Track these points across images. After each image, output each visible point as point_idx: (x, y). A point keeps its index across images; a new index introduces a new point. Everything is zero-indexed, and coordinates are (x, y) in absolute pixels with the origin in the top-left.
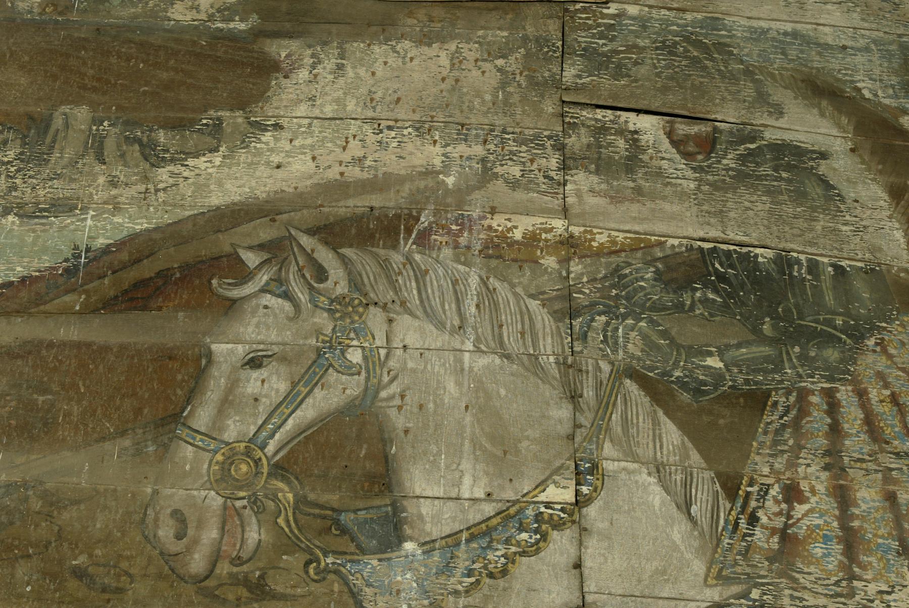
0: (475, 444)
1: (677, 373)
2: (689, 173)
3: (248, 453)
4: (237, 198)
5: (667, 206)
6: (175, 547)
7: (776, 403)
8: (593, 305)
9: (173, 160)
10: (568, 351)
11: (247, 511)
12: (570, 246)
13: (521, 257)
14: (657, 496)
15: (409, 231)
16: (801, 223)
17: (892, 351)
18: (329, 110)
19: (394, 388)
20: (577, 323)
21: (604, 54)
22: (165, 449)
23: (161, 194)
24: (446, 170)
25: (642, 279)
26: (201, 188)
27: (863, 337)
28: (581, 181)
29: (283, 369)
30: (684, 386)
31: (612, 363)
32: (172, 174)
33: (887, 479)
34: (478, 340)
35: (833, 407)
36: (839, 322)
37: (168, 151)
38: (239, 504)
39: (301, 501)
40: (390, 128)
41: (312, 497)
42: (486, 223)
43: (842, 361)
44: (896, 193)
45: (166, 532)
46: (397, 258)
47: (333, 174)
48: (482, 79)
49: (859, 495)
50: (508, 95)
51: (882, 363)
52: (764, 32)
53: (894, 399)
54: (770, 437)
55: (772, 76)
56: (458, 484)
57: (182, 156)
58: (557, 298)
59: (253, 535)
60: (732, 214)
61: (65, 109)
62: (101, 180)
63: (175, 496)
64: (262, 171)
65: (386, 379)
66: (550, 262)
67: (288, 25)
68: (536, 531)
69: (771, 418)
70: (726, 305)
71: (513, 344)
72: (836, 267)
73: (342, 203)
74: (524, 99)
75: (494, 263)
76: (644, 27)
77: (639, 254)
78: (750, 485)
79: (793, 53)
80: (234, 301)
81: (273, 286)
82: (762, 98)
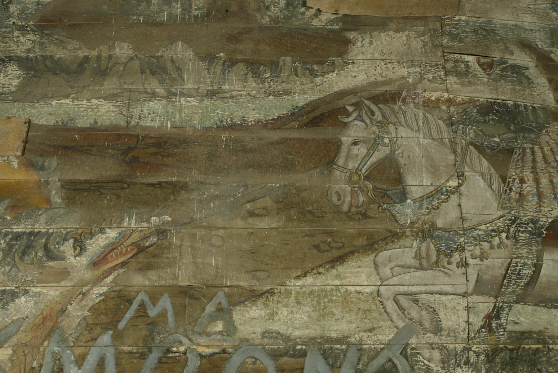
0: (426, 168)
1: (486, 143)
2: (485, 76)
3: (356, 173)
4: (343, 88)
5: (479, 87)
6: (338, 203)
7: (516, 152)
8: (458, 121)
9: (320, 75)
10: (452, 137)
11: (359, 191)
12: (450, 102)
13: (435, 106)
14: (482, 183)
15: (399, 98)
16: (521, 92)
17: (550, 134)
18: (369, 57)
19: (400, 151)
20: (454, 127)
21: (455, 34)
22: (330, 173)
23: (318, 87)
24: (409, 77)
25: (473, 112)
26: (330, 85)
27: (541, 130)
28: (452, 79)
29: (364, 145)
30: (488, 147)
31: (465, 141)
32: (321, 80)
33: (550, 176)
34: (424, 134)
35: (533, 153)
36: (534, 125)
37: (318, 72)
38: (356, 189)
39: (375, 188)
40: (389, 63)
41: (378, 186)
42: (423, 95)
43: (535, 138)
44: (550, 81)
45: (335, 199)
46: (396, 107)
47: (373, 79)
48: (417, 44)
49: (542, 181)
50: (426, 50)
51: (547, 138)
52: (506, 25)
53: (551, 150)
54: (515, 163)
55: (509, 40)
56: (422, 181)
58: (447, 119)
59: (361, 199)
60: (500, 90)
61: (283, 58)
62: (298, 83)
63: (336, 187)
64: (350, 78)
65: (397, 148)
66: (444, 107)
67: (352, 27)
68: (447, 195)
69: (515, 157)
70: (499, 121)
71: (435, 135)
72: (532, 107)
73: (377, 89)
74: (431, 51)
75: (427, 108)
76: (467, 24)
77: (471, 104)
78: (510, 179)
79: (516, 32)
80: (346, 123)
81: (358, 118)
82: (507, 49)
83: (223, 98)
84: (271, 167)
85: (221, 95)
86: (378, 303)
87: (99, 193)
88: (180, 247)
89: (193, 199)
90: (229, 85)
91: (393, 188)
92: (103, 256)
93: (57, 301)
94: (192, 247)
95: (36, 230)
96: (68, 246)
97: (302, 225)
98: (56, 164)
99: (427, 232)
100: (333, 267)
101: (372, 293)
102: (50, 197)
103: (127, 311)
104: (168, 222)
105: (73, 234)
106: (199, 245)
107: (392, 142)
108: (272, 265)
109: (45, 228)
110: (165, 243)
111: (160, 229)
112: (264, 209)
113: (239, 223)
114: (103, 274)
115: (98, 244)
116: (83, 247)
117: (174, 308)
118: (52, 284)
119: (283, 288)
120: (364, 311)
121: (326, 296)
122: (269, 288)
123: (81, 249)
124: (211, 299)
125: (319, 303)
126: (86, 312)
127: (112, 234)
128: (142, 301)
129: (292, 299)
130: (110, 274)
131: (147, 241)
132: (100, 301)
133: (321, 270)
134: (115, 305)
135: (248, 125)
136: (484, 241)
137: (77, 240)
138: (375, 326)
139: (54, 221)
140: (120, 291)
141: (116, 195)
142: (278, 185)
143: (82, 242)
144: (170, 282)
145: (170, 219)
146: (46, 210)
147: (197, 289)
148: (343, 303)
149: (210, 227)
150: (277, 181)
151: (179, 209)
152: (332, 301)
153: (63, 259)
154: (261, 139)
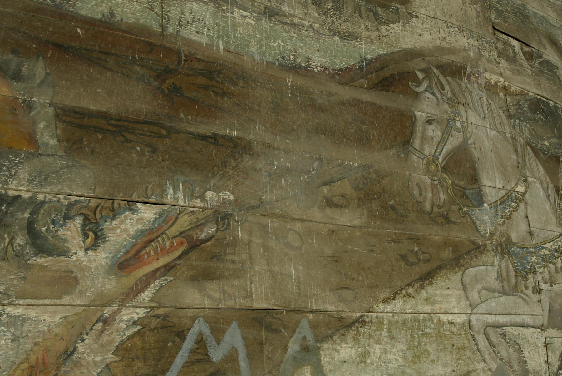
4: (411, 47)
6: (420, 199)
9: (385, 23)
11: (438, 186)
14: (542, 193)
18: (432, 13)
23: (384, 38)
32: (387, 30)
37: (382, 18)
39: (453, 183)
40: (451, 27)
41: (456, 182)
45: (416, 192)
47: (438, 42)
52: (537, 14)
56: (495, 182)
57: (389, 22)
64: (416, 36)
65: (469, 136)
73: (444, 57)
81: (429, 88)
83: (283, 23)
84: (344, 137)
85: (280, 18)
86: (470, 337)
87: (122, 139)
88: (249, 244)
89: (260, 169)
90: (288, 7)
91: (470, 187)
92: (134, 251)
93: (56, 335)
94: (264, 246)
95: (11, 193)
96: (73, 228)
97: (386, 225)
98: (43, 73)
99: (505, 248)
100: (422, 287)
101: (463, 325)
102: (35, 133)
103: (177, 353)
104: (230, 202)
105: (81, 208)
106: (272, 243)
107: (464, 129)
108: (358, 280)
109: (28, 191)
110: (228, 237)
111: (220, 213)
112: (343, 196)
113: (316, 214)
114: (137, 285)
115: (126, 230)
116: (99, 234)
117: (247, 346)
118: (47, 301)
119: (374, 315)
120: (459, 349)
121: (419, 328)
122: (358, 315)
123: (97, 237)
124: (294, 332)
125: (413, 337)
126: (111, 355)
127: (148, 213)
128: (201, 334)
129: (385, 332)
130: (147, 286)
131: (202, 231)
132: (133, 335)
133: (411, 291)
134: (157, 341)
135: (313, 71)
136: (551, 263)
137: (89, 220)
138: (471, 369)
139: (46, 179)
140: (165, 317)
141: (150, 146)
142: (356, 165)
143: (97, 223)
144: (241, 303)
145: (232, 197)
146: (29, 157)
147: (275, 316)
148: (437, 338)
149: (283, 217)
150: (354, 159)
151: (243, 183)
152: (425, 335)
153: (65, 253)
154: (330, 94)
